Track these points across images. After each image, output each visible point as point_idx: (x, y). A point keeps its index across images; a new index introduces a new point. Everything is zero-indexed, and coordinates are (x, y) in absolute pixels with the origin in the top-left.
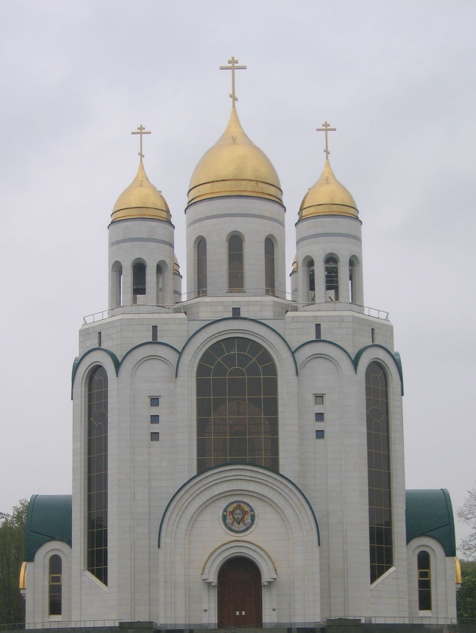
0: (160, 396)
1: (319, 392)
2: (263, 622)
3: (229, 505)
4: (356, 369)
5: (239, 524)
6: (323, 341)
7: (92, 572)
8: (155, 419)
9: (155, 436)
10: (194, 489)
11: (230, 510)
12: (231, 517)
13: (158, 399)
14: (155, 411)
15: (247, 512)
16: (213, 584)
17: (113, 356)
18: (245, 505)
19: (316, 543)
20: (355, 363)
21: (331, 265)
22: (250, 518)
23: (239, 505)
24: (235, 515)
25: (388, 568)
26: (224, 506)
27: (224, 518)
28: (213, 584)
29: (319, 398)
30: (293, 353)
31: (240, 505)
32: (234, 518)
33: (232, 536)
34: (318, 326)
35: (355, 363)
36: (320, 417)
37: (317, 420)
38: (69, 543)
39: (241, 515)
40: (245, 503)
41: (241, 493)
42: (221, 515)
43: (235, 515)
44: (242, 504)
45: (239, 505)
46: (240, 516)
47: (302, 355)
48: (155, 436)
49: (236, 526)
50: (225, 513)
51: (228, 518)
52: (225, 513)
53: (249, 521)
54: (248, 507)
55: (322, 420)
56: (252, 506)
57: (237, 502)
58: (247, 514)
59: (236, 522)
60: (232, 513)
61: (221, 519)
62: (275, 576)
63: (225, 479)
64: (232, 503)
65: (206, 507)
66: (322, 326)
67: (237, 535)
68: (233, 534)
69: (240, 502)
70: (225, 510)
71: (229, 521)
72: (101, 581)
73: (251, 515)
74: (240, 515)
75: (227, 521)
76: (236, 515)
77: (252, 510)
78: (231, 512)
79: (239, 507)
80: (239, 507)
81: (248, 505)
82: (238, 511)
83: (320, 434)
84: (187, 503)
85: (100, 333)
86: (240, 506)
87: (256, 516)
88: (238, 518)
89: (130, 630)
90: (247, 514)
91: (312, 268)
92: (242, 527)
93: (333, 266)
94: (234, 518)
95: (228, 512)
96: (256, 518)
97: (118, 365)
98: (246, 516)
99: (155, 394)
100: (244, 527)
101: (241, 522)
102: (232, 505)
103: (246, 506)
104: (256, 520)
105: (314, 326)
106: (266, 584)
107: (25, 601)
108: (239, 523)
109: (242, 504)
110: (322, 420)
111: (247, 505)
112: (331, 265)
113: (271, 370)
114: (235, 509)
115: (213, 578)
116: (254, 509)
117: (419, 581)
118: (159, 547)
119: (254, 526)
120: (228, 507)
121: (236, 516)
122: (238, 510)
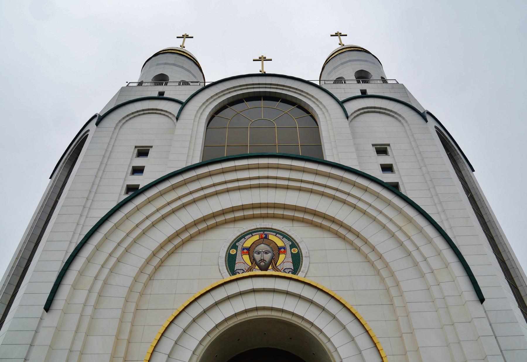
0: (151, 147)
1: (381, 141)
3: (243, 236)
11: (245, 245)
12: (246, 258)
15: (284, 248)
18: (277, 235)
19: (470, 294)
22: (291, 260)
24: (255, 255)
31: (266, 235)
32: (254, 259)
39: (270, 254)
41: (271, 211)
42: (223, 254)
43: (255, 255)
45: (264, 236)
46: (268, 257)
52: (233, 252)
54: (284, 239)
56: (293, 236)
57: (261, 231)
58: (285, 252)
59: (257, 267)
60: (248, 251)
63: (236, 184)
64: (251, 233)
65: (191, 238)
69: (267, 231)
70: (234, 245)
73: (292, 253)
74: (266, 253)
76: (259, 253)
77: (294, 245)
78: (248, 249)
79: (264, 239)
80: (264, 239)
81: (285, 235)
82: (262, 247)
84: (148, 223)
86: (266, 237)
87: (303, 255)
88: (262, 260)
90: (285, 252)
94: (253, 260)
95: (239, 248)
96: (304, 258)
98: (282, 257)
101: (270, 267)
102: (250, 235)
103: (281, 237)
104: (305, 262)
111: (281, 235)
114: (255, 244)
116: (298, 241)
118: (47, 308)
120: (241, 239)
121: (257, 257)
122: (262, 245)
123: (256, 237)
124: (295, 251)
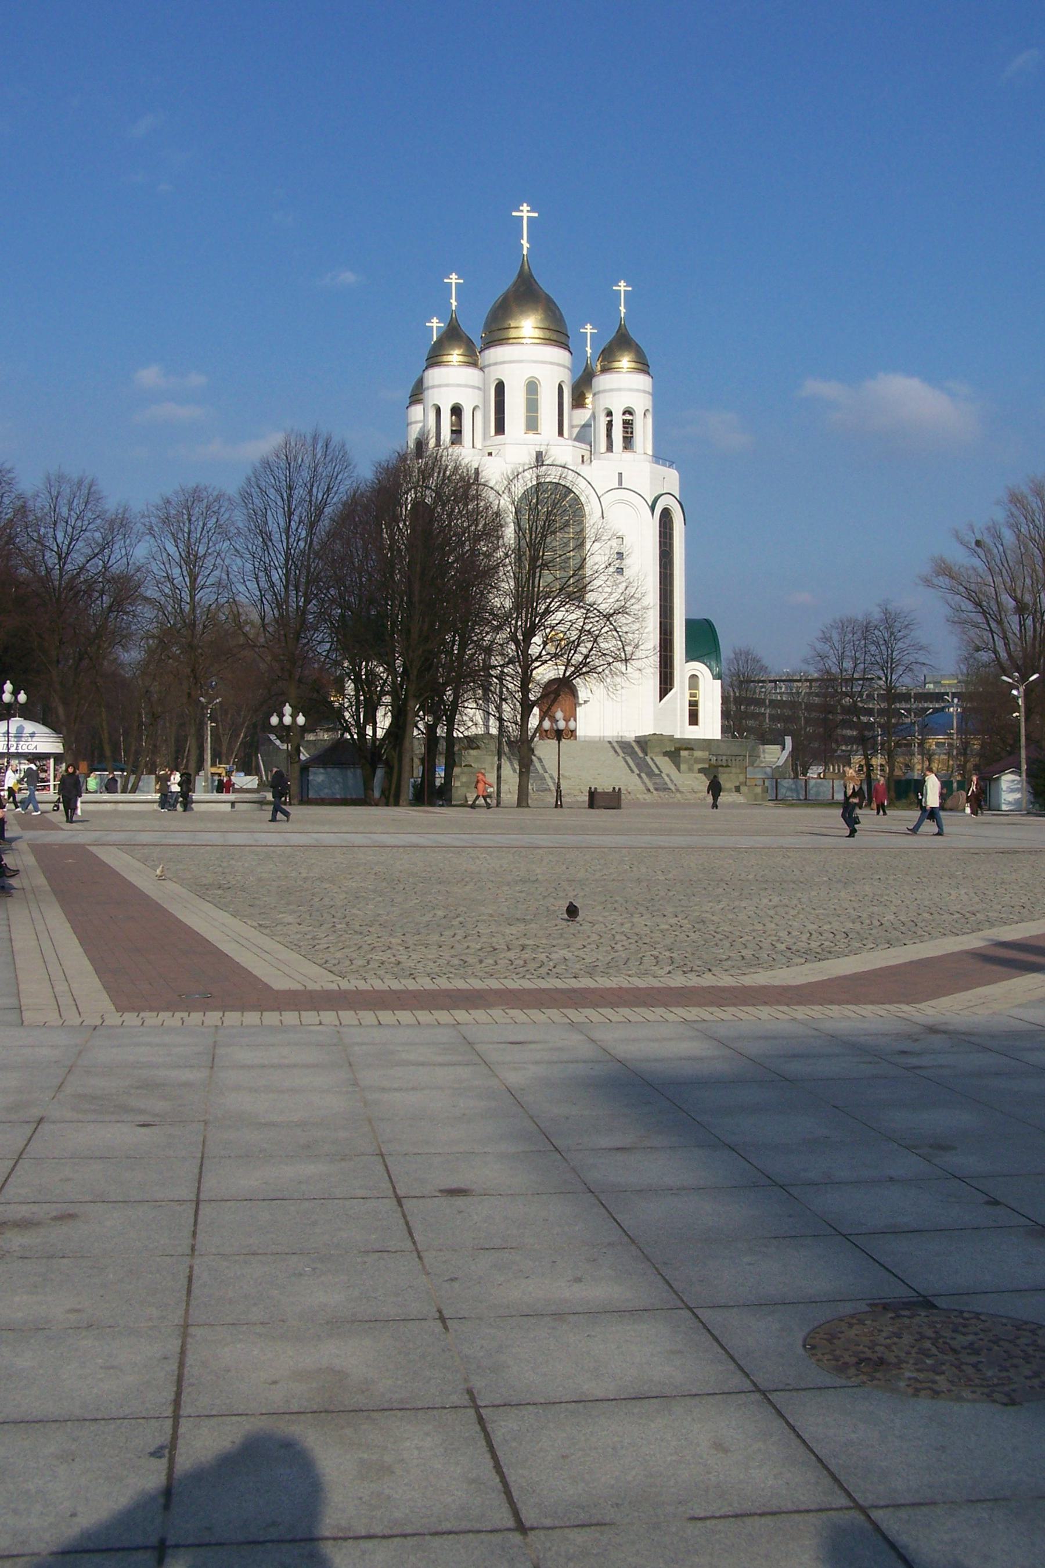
4: (653, 514)
20: (652, 508)
21: (628, 417)
25: (671, 690)
30: (599, 498)
34: (620, 474)
35: (652, 508)
112: (628, 417)
117: (690, 701)
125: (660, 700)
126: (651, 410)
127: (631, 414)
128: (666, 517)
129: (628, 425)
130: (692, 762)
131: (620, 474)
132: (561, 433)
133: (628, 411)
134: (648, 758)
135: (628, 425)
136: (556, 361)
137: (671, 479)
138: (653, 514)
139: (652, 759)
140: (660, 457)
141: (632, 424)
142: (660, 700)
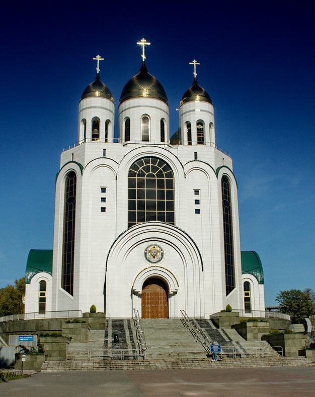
2: (169, 316)
4: (217, 177)
5: (154, 258)
6: (198, 161)
7: (64, 288)
8: (103, 200)
9: (103, 209)
10: (129, 235)
13: (105, 189)
14: (103, 195)
16: (139, 293)
17: (79, 164)
19: (201, 269)
23: (154, 246)
25: (233, 288)
26: (146, 247)
27: (146, 254)
28: (139, 293)
29: (197, 192)
33: (148, 265)
34: (196, 153)
35: (217, 174)
36: (197, 202)
37: (196, 203)
38: (49, 270)
40: (156, 245)
44: (156, 247)
47: (188, 167)
48: (103, 209)
49: (152, 259)
50: (146, 252)
51: (147, 255)
52: (146, 252)
53: (160, 256)
55: (198, 203)
61: (144, 255)
62: (177, 288)
64: (150, 246)
66: (198, 154)
67: (154, 265)
68: (151, 264)
71: (149, 255)
72: (69, 293)
75: (147, 256)
83: (198, 211)
85: (73, 154)
89: (90, 318)
91: (189, 128)
92: (156, 259)
93: (202, 127)
94: (151, 254)
97: (82, 168)
99: (104, 186)
100: (158, 260)
105: (194, 153)
106: (172, 293)
107: (24, 305)
108: (154, 258)
109: (156, 247)
110: (198, 203)
113: (171, 175)
115: (139, 288)
119: (163, 260)
121: (152, 254)
123: (152, 247)
124: (162, 252)
125: (227, 295)
126: (213, 123)
127: (202, 125)
128: (225, 180)
129: (200, 132)
130: (256, 331)
131: (196, 153)
132: (163, 140)
133: (200, 123)
134: (220, 330)
135: (200, 132)
136: (159, 107)
137: (229, 162)
138: (217, 177)
139: (223, 330)
140: (220, 145)
141: (203, 130)
142: (227, 295)
